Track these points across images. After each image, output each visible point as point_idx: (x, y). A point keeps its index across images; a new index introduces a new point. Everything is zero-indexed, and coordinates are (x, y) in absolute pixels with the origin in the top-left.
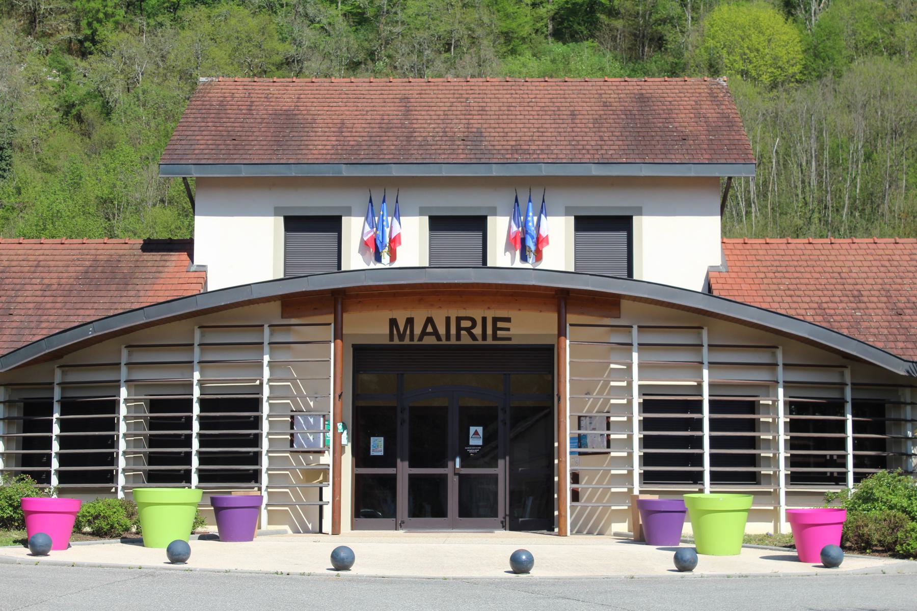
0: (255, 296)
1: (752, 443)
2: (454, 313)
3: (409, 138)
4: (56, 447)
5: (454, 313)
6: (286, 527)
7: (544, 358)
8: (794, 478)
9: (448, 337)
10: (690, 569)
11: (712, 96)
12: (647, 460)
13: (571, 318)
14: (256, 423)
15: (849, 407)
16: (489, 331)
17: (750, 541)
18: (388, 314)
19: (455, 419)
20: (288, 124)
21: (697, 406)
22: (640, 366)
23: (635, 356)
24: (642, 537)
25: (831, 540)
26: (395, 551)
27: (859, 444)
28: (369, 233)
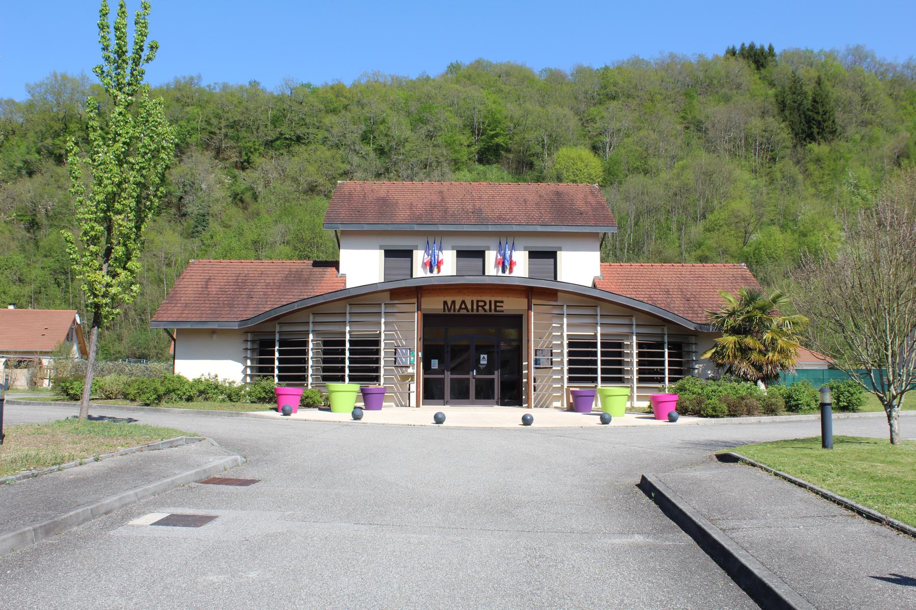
0: (379, 289)
1: (620, 363)
2: (475, 299)
3: (446, 211)
4: (277, 363)
5: (475, 299)
6: (393, 404)
7: (517, 321)
8: (640, 380)
9: (472, 310)
10: (607, 423)
11: (592, 193)
12: (570, 371)
13: (534, 301)
14: (377, 352)
15: (666, 345)
16: (493, 307)
17: (631, 410)
18: (441, 299)
19: (475, 351)
20: (384, 204)
21: (594, 345)
22: (568, 325)
23: (565, 320)
24: (572, 408)
25: (671, 408)
26: (459, 415)
27: (670, 363)
28: (427, 258)
